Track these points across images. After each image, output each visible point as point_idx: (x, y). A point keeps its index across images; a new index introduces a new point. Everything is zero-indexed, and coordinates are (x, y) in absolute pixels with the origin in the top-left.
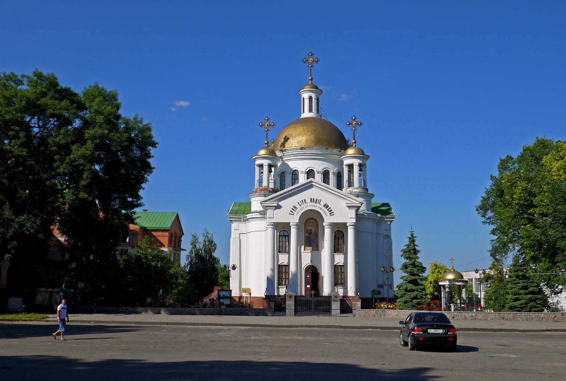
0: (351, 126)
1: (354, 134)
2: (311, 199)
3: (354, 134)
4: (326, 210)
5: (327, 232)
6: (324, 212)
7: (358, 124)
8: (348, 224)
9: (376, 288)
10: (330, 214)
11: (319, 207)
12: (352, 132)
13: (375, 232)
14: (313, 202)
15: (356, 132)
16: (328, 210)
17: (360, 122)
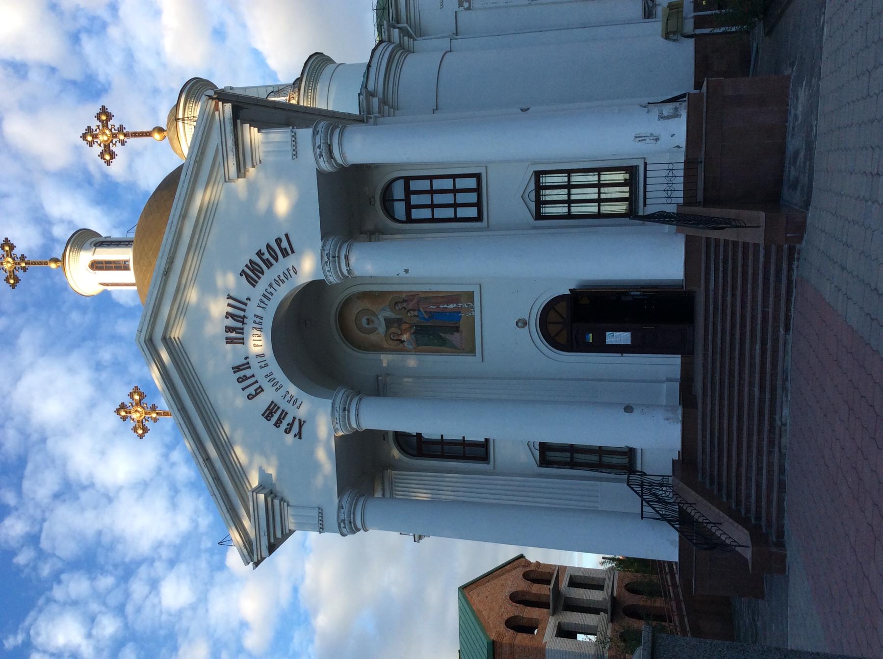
0: (112, 148)
1: (135, 135)
2: (230, 341)
3: (135, 135)
4: (269, 275)
5: (374, 264)
6: (279, 281)
7: (105, 125)
8: (326, 167)
9: (656, 26)
10: (285, 254)
11: (262, 305)
12: (131, 141)
13: (445, 43)
14: (240, 331)
15: (127, 129)
16: (269, 265)
17: (98, 116)
